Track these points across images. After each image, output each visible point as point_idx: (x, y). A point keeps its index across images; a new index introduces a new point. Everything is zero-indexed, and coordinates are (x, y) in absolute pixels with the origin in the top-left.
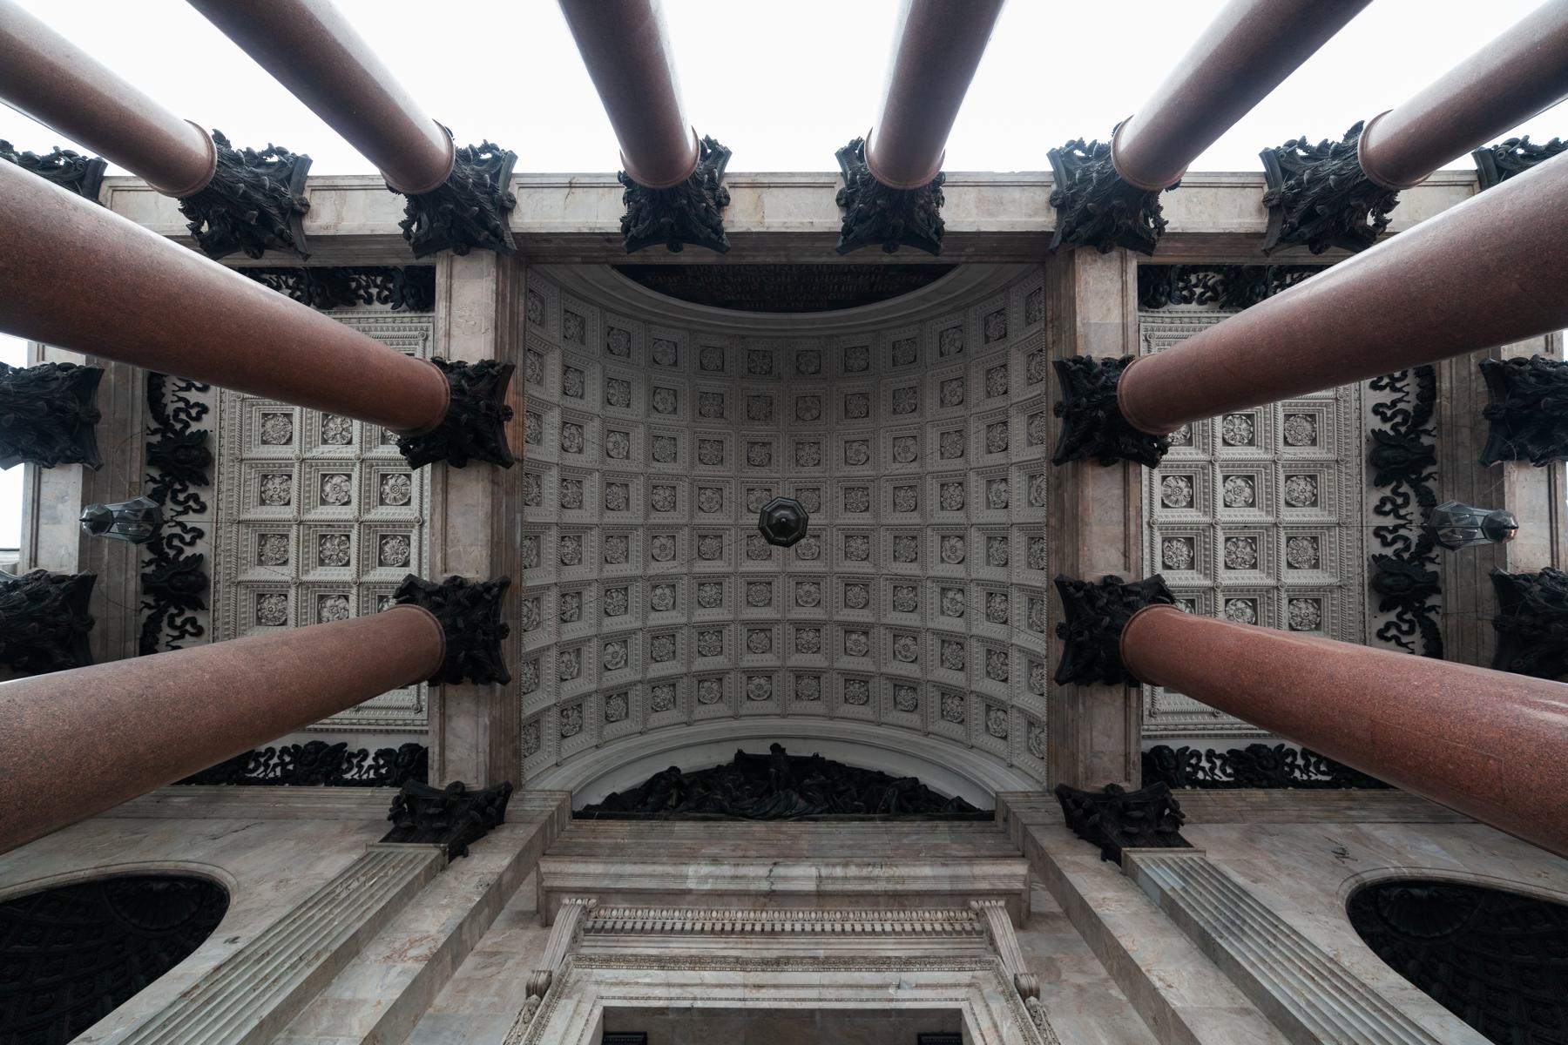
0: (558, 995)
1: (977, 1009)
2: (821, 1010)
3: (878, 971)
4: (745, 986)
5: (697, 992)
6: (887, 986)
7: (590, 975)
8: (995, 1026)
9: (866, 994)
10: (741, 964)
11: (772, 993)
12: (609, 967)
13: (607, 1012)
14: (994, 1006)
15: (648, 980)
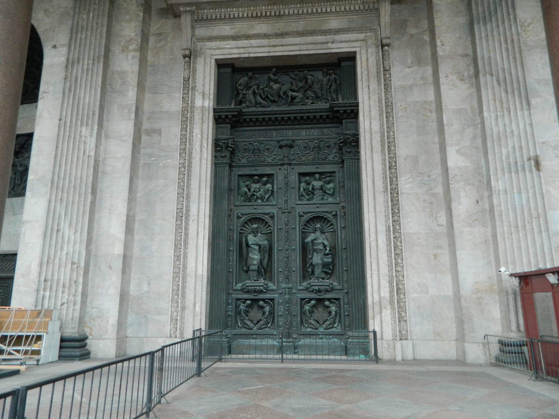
0: (196, 57)
1: (362, 52)
2: (300, 55)
3: (325, 35)
4: (269, 46)
5: (250, 50)
6: (327, 43)
7: (205, 45)
8: (367, 59)
9: (319, 46)
10: (266, 36)
11: (280, 48)
12: (212, 41)
13: (216, 60)
14: (370, 50)
15: (229, 46)
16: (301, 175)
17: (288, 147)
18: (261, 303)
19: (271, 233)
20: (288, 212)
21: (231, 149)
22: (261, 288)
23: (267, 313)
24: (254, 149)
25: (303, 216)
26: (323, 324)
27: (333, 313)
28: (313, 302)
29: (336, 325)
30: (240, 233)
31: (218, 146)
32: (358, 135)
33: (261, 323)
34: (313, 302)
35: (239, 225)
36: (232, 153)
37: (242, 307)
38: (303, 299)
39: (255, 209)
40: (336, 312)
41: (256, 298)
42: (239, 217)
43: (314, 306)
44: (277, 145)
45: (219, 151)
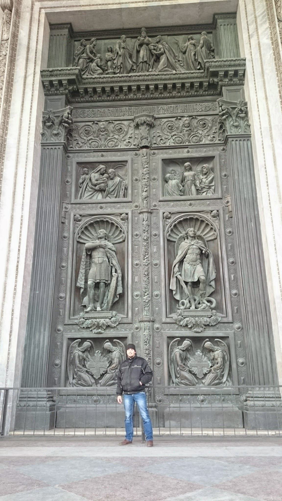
16: (167, 162)
17: (148, 124)
18: (108, 345)
19: (124, 241)
20: (147, 212)
21: (66, 125)
22: (108, 320)
23: (116, 361)
24: (99, 130)
25: (169, 218)
26: (203, 378)
27: (220, 360)
28: (186, 343)
29: (224, 379)
30: (78, 242)
31: (47, 122)
32: (246, 104)
33: (107, 376)
34: (186, 343)
35: (76, 231)
36: (69, 133)
37: (77, 352)
38: (171, 338)
39: (101, 208)
40: (224, 358)
41: (100, 336)
42: (76, 220)
43: (187, 350)
44: (132, 125)
45: (49, 127)
